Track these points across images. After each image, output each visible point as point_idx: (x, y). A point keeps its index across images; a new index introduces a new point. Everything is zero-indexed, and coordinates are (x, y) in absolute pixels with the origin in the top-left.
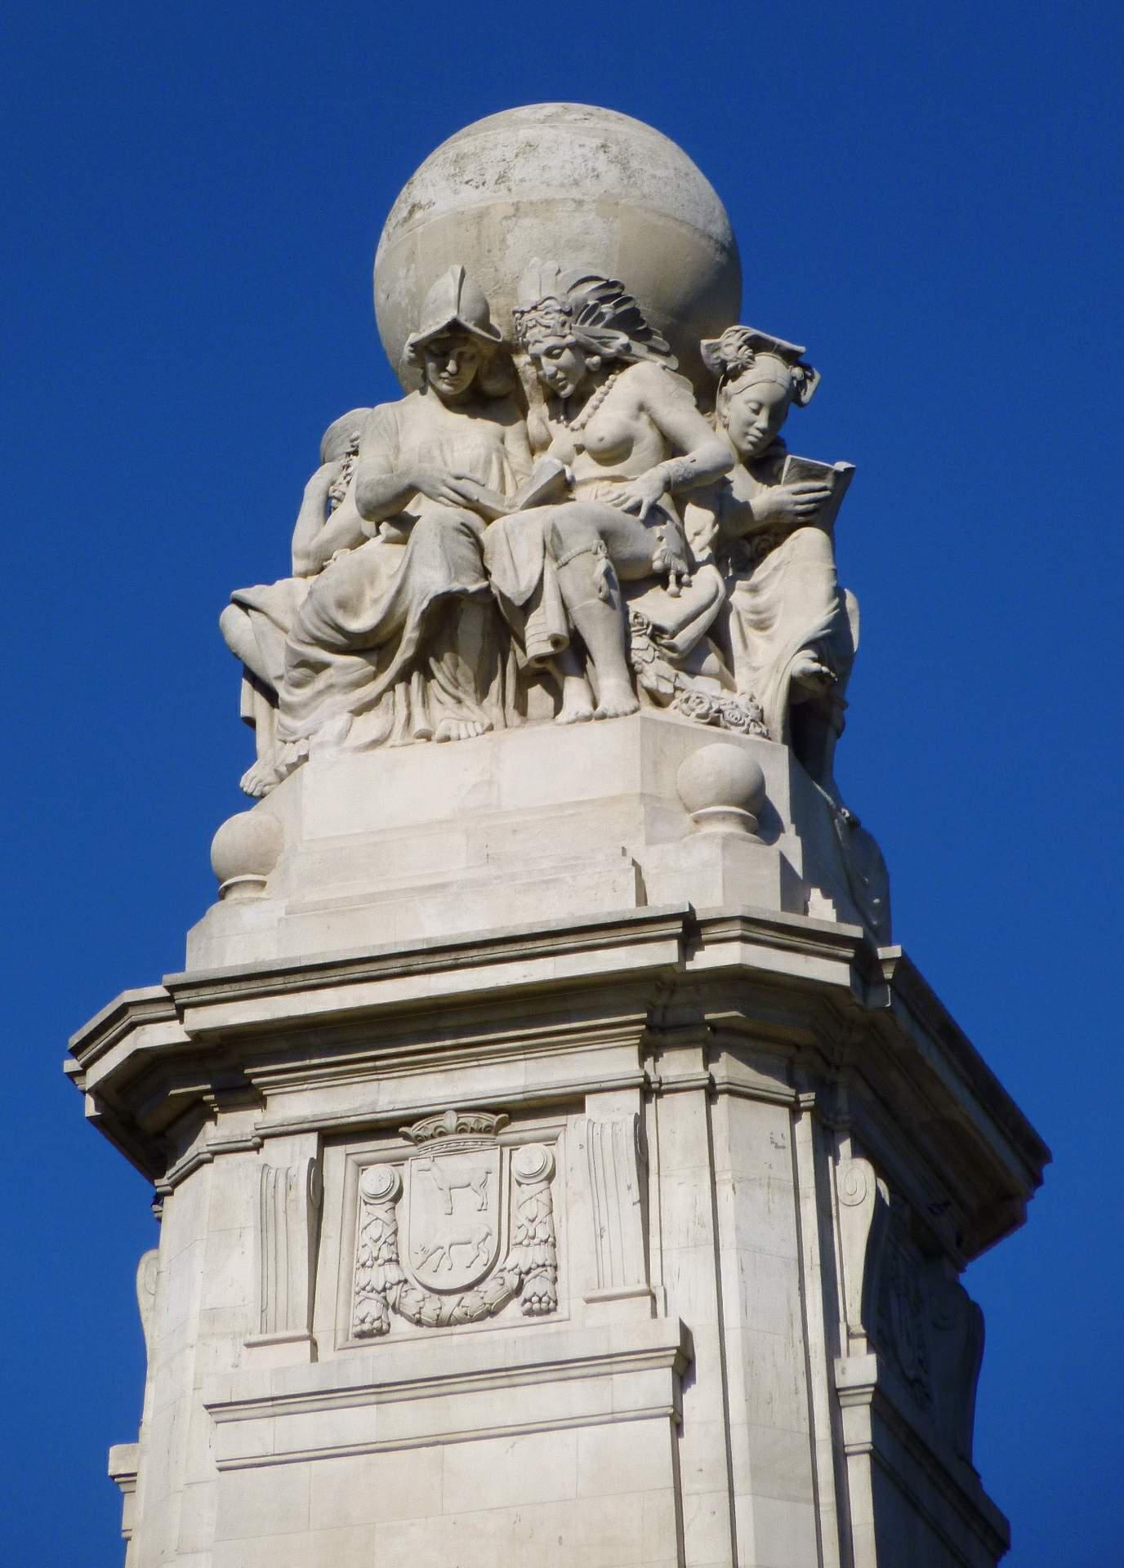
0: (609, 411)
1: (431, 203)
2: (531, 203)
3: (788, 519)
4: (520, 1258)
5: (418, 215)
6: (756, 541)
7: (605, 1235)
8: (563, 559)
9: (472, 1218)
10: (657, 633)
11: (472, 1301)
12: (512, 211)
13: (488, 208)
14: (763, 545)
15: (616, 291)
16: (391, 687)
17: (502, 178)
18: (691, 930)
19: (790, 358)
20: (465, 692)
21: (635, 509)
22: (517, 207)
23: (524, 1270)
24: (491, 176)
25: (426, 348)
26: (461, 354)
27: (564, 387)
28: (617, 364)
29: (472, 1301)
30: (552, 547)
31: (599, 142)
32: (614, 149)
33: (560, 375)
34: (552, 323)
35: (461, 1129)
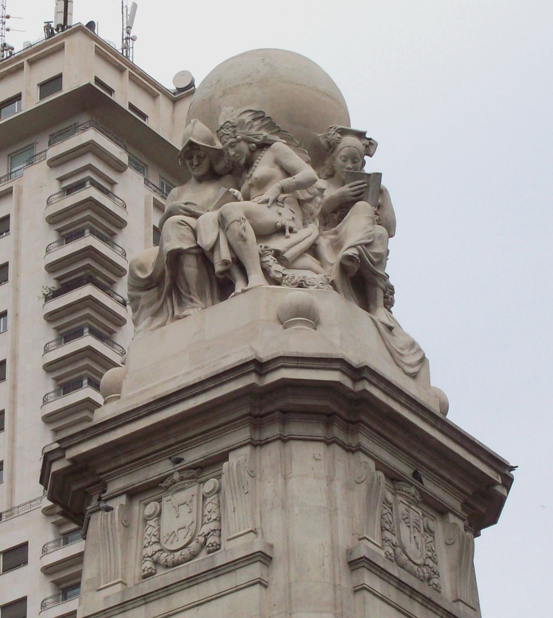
2: (230, 89)
4: (205, 529)
7: (236, 511)
8: (226, 227)
9: (186, 517)
11: (185, 552)
13: (213, 96)
14: (342, 213)
15: (261, 115)
16: (165, 301)
18: (259, 366)
20: (194, 296)
22: (224, 92)
23: (206, 533)
27: (240, 159)
28: (264, 145)
33: (238, 155)
34: (229, 132)
35: (182, 479)
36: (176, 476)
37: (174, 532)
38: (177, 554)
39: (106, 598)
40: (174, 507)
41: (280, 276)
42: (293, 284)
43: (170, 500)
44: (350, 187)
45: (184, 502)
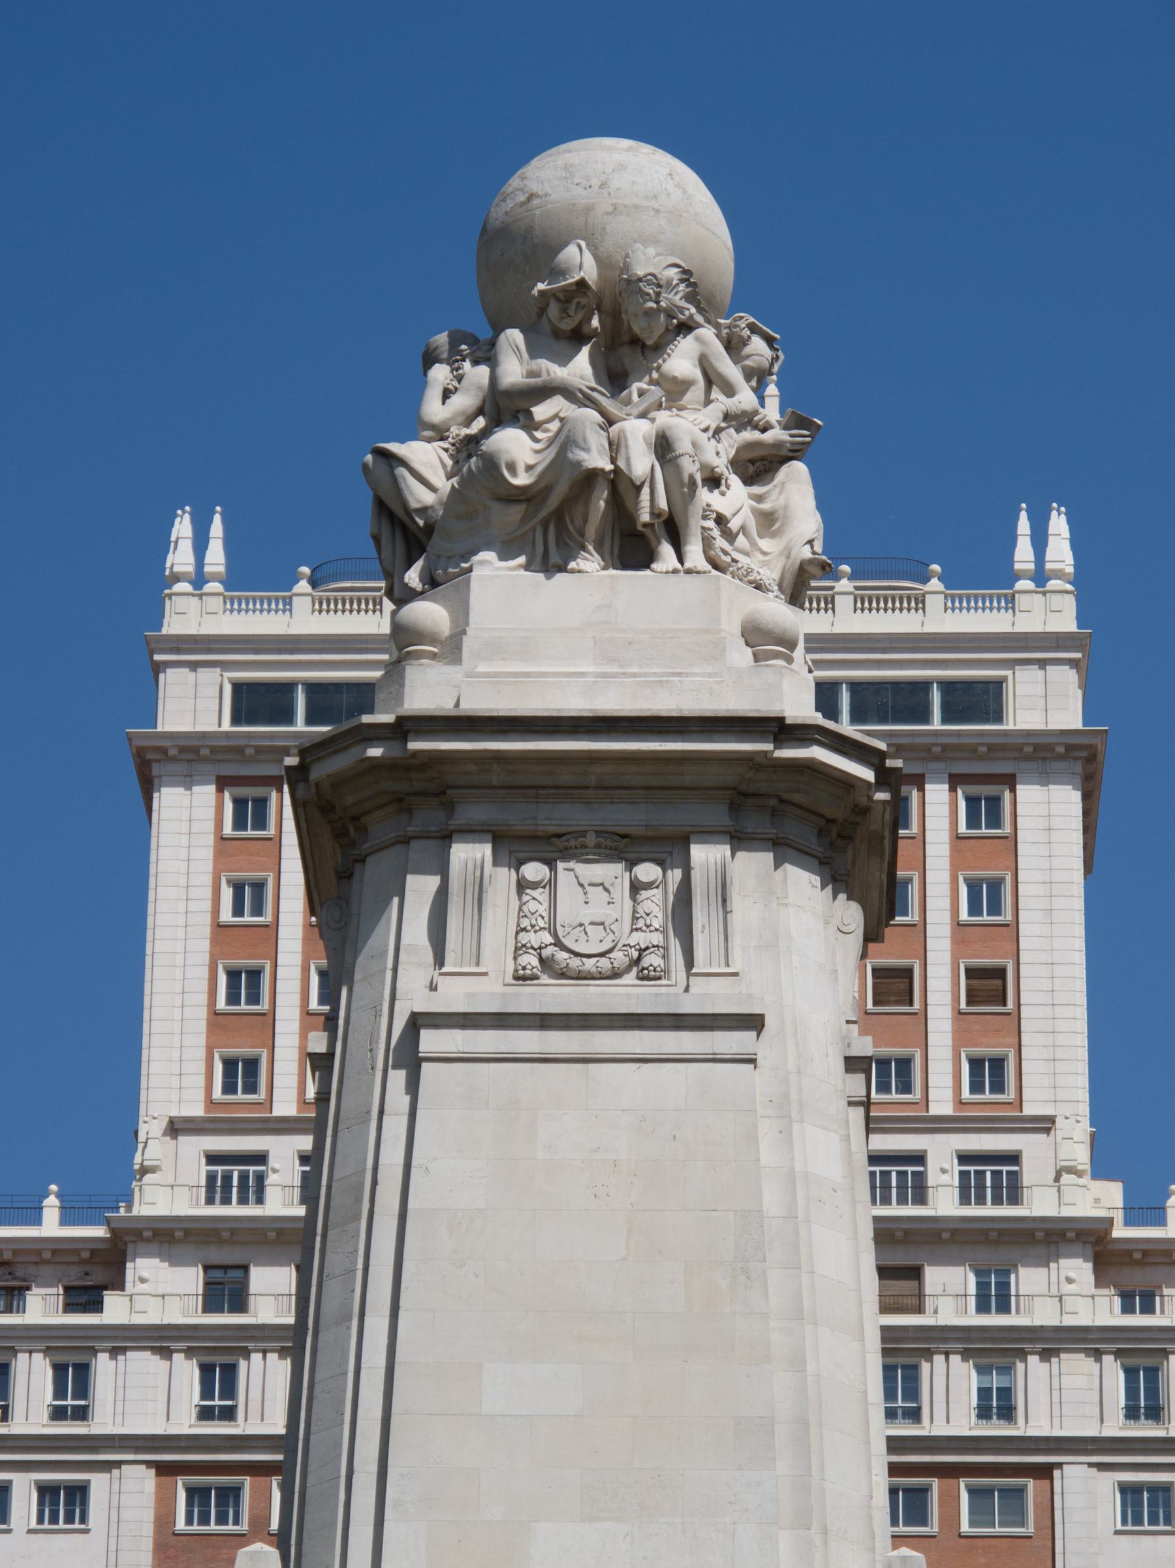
0: (681, 360)
1: (546, 195)
3: (784, 452)
5: (536, 202)
6: (758, 464)
10: (721, 520)
11: (604, 963)
12: (611, 209)
17: (603, 185)
18: (781, 730)
19: (770, 341)
21: (705, 430)
22: (615, 206)
23: (643, 947)
24: (595, 182)
25: (554, 295)
26: (578, 303)
28: (686, 328)
29: (604, 963)
30: (663, 447)
31: (667, 171)
32: (677, 178)
34: (651, 292)
35: (598, 846)
36: (591, 840)
37: (581, 925)
38: (563, 955)
39: (469, 996)
40: (581, 885)
41: (728, 559)
42: (750, 582)
43: (572, 870)
44: (791, 436)
45: (600, 881)
